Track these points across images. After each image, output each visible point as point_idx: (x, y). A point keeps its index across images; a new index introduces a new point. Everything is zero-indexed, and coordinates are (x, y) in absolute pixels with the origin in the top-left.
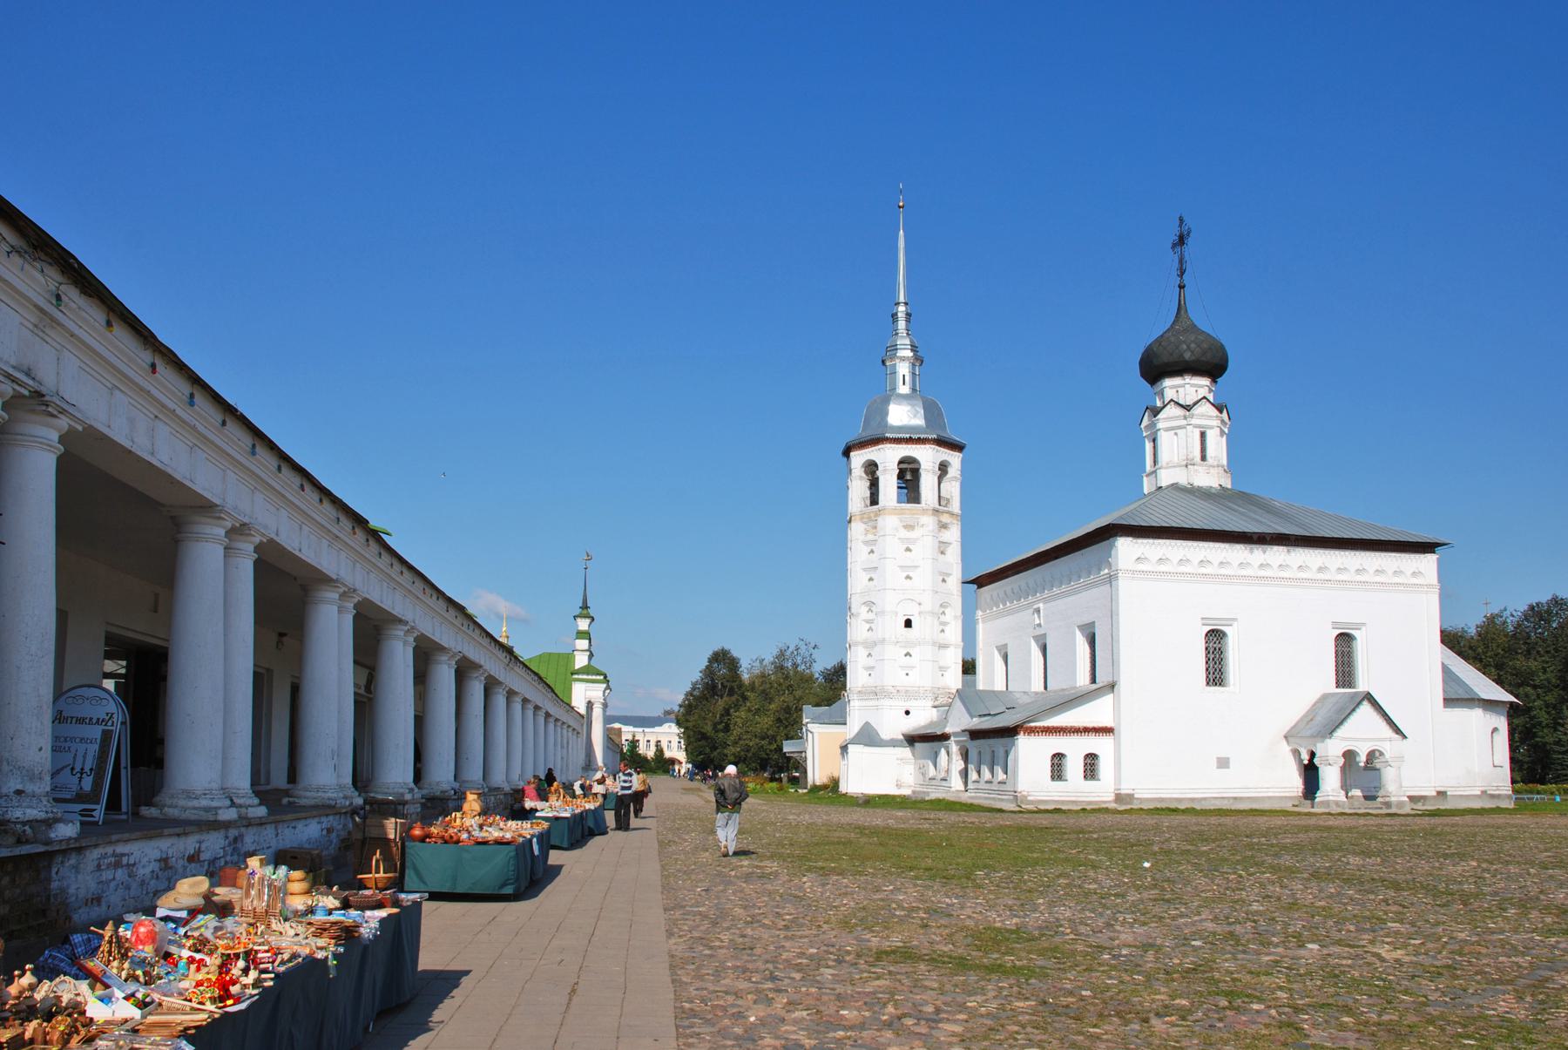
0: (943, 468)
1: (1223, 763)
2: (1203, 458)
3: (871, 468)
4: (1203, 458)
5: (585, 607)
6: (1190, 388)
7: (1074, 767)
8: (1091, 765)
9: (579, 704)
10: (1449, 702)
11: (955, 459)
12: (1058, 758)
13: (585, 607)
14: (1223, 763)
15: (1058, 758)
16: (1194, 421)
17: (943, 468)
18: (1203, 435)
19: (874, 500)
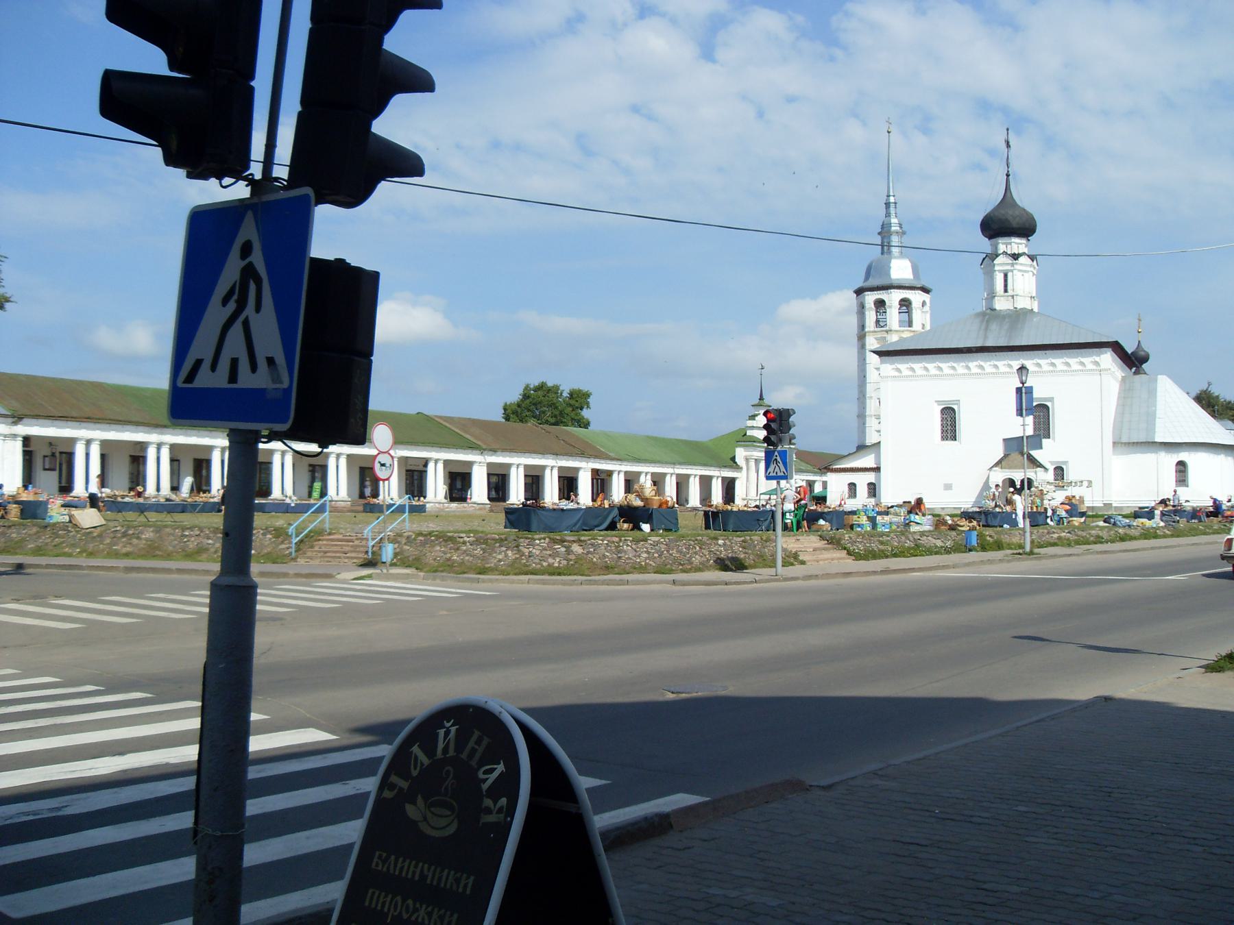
0: (905, 304)
1: (948, 487)
2: (1006, 291)
3: (862, 307)
4: (1006, 291)
5: (761, 398)
6: (1017, 244)
7: (862, 491)
8: (873, 489)
9: (740, 460)
10: (1114, 443)
11: (916, 297)
12: (852, 486)
13: (761, 398)
14: (948, 487)
15: (852, 486)
16: (997, 268)
17: (905, 304)
18: (1006, 276)
19: (862, 327)
